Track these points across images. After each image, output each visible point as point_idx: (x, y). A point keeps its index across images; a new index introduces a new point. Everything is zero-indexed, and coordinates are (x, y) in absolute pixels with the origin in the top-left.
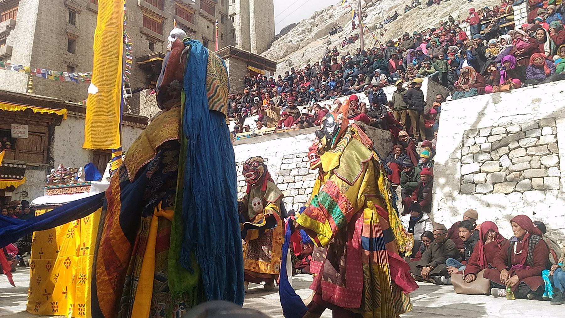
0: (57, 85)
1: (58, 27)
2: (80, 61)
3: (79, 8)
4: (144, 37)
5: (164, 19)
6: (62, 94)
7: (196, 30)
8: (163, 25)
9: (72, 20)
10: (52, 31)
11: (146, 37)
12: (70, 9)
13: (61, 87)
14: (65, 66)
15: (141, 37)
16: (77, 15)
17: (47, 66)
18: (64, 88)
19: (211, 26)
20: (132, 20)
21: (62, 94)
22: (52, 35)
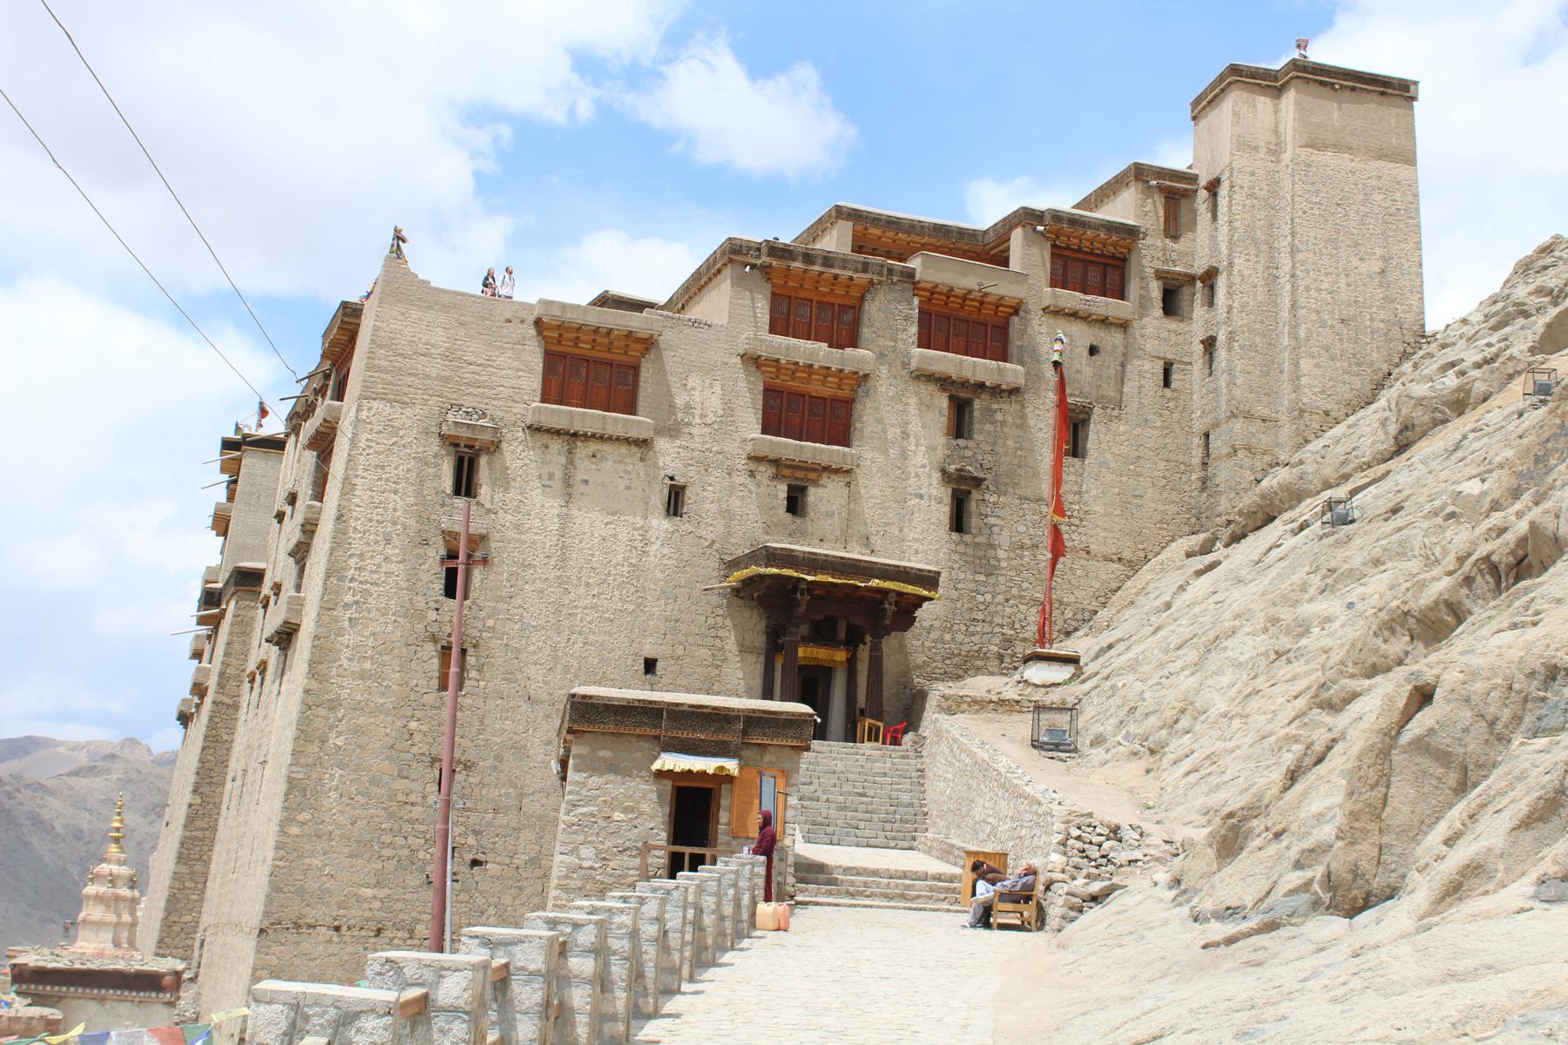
0: (399, 723)
1: (412, 522)
2: (490, 622)
4: (765, 471)
5: (861, 379)
6: (415, 750)
7: (1021, 381)
8: (853, 400)
9: (465, 484)
10: (388, 541)
11: (771, 470)
12: (457, 445)
13: (413, 725)
14: (430, 652)
15: (752, 474)
16: (483, 461)
17: (368, 665)
18: (425, 728)
19: (1111, 340)
20: (710, 419)
21: (415, 750)
22: (389, 551)
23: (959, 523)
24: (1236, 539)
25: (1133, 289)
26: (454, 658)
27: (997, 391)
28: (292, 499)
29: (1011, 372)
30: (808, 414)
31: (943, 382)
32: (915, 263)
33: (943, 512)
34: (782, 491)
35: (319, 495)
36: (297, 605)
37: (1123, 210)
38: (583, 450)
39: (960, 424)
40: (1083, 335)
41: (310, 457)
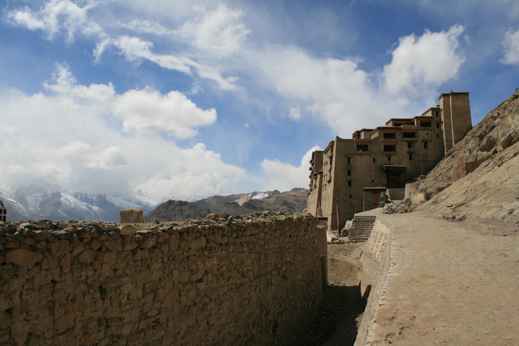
3: (350, 156)
9: (349, 162)
19: (430, 132)
23: (411, 159)
24: (447, 157)
25: (432, 125)
26: (350, 184)
27: (414, 141)
28: (327, 163)
29: (415, 139)
30: (390, 149)
31: (407, 141)
32: (402, 126)
33: (408, 158)
34: (387, 158)
35: (331, 164)
36: (330, 178)
37: (430, 114)
38: (362, 156)
39: (409, 146)
40: (425, 132)
41: (329, 159)
